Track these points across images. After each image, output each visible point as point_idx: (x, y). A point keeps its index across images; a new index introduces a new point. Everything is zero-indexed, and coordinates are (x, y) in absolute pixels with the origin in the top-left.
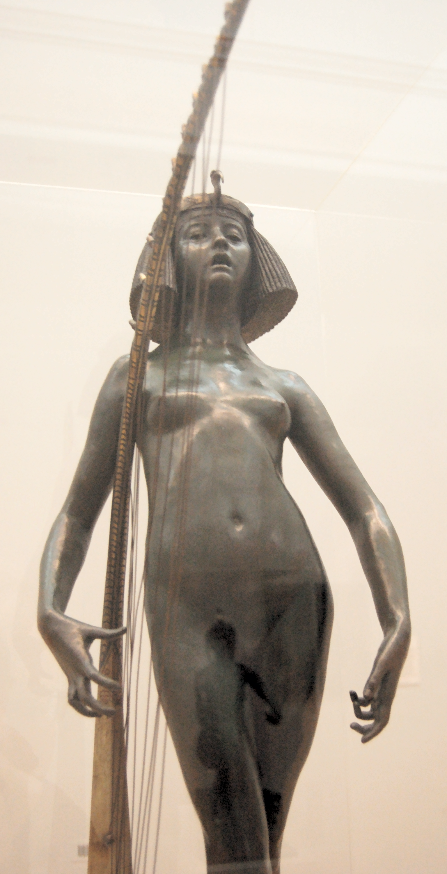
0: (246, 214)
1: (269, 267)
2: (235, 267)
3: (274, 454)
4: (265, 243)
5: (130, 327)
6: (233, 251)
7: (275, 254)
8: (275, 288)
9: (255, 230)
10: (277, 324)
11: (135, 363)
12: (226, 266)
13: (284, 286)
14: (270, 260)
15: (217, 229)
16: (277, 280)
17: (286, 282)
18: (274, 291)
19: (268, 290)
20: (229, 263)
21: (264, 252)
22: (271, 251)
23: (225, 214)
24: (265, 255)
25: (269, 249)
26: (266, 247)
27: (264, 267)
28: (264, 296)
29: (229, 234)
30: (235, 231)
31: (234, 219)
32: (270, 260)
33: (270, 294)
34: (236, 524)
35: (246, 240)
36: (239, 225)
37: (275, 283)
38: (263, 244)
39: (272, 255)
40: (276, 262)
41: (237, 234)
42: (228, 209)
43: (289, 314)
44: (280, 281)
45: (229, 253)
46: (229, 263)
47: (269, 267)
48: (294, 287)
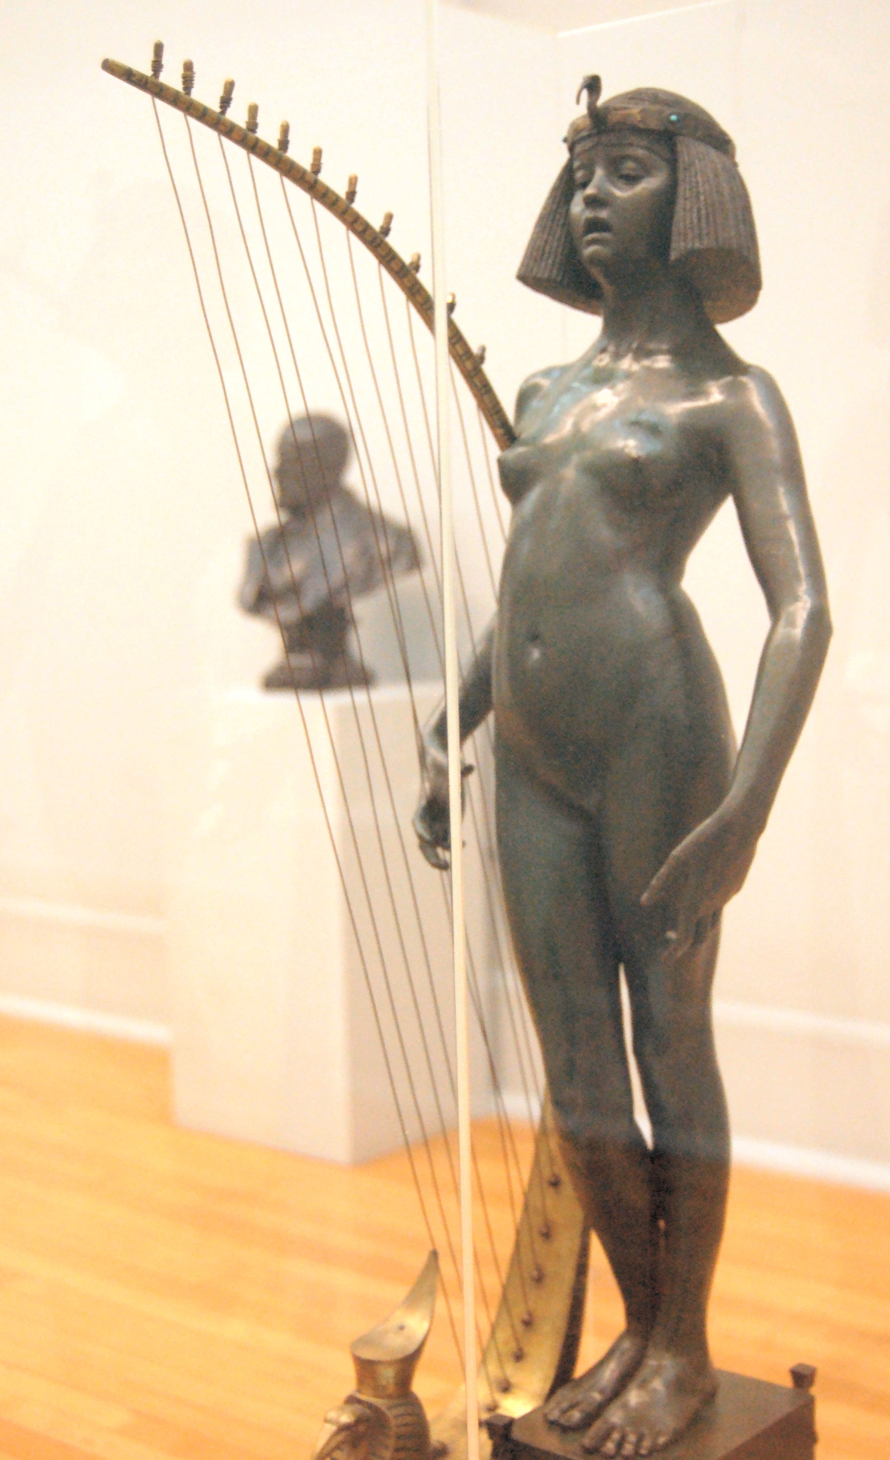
45: (604, 214)
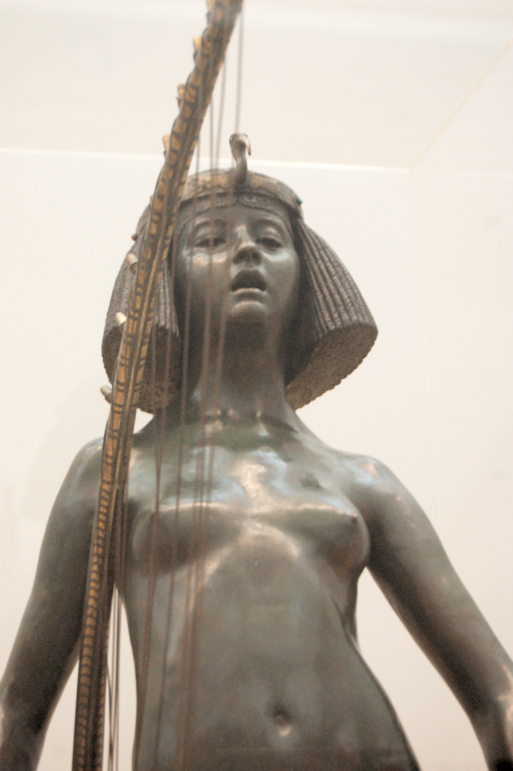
0: (289, 201)
1: (328, 287)
2: (270, 292)
3: (342, 604)
4: (323, 247)
5: (103, 397)
6: (269, 266)
7: (338, 265)
8: (339, 323)
9: (305, 226)
10: (345, 376)
11: (111, 457)
12: (257, 290)
13: (355, 318)
14: (331, 276)
15: (241, 230)
16: (342, 308)
17: (356, 312)
18: (338, 327)
19: (327, 327)
20: (262, 285)
21: (320, 262)
22: (332, 259)
23: (255, 203)
24: (323, 267)
25: (328, 256)
26: (322, 253)
27: (320, 286)
28: (321, 335)
29: (262, 236)
30: (272, 230)
31: (270, 211)
32: (331, 276)
33: (331, 333)
34: (281, 724)
35: (290, 244)
36: (278, 220)
37: (340, 315)
38: (318, 250)
39: (334, 267)
40: (340, 278)
41: (275, 236)
42: (259, 195)
43: (365, 360)
44: (347, 310)
45: (261, 269)
46: (262, 285)
47: (328, 287)
48: (371, 318)
